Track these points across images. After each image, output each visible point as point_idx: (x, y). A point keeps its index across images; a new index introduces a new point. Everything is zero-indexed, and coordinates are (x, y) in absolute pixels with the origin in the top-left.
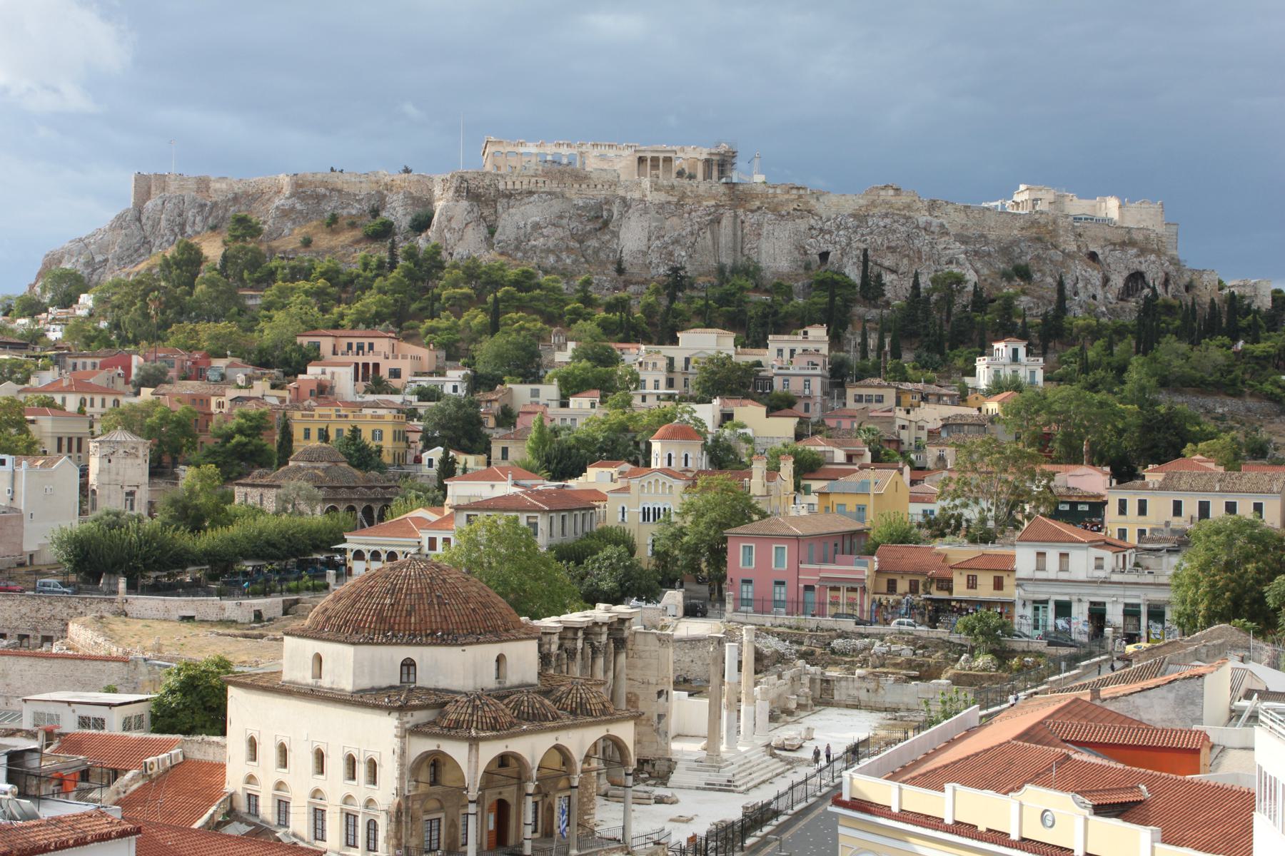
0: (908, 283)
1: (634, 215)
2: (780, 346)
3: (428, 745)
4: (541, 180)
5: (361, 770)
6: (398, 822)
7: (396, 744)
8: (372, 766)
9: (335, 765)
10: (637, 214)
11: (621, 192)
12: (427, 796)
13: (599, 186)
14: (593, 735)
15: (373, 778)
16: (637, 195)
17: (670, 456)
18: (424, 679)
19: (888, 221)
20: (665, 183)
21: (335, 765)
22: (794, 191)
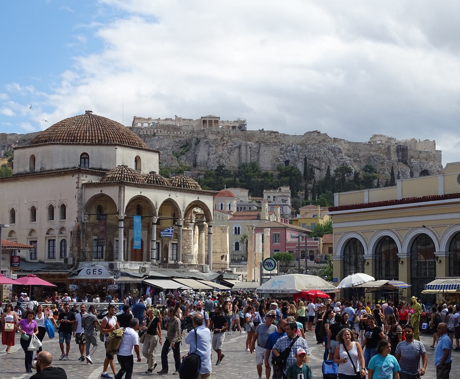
0: (324, 173)
1: (202, 144)
2: (269, 195)
3: (96, 191)
4: (159, 130)
5: (57, 212)
6: (79, 238)
7: (76, 192)
8: (63, 207)
9: (43, 213)
11: (195, 135)
12: (94, 226)
14: (190, 199)
15: (64, 216)
16: (202, 136)
17: (222, 204)
18: (93, 163)
19: (315, 146)
20: (215, 130)
21: (43, 213)
22: (273, 134)
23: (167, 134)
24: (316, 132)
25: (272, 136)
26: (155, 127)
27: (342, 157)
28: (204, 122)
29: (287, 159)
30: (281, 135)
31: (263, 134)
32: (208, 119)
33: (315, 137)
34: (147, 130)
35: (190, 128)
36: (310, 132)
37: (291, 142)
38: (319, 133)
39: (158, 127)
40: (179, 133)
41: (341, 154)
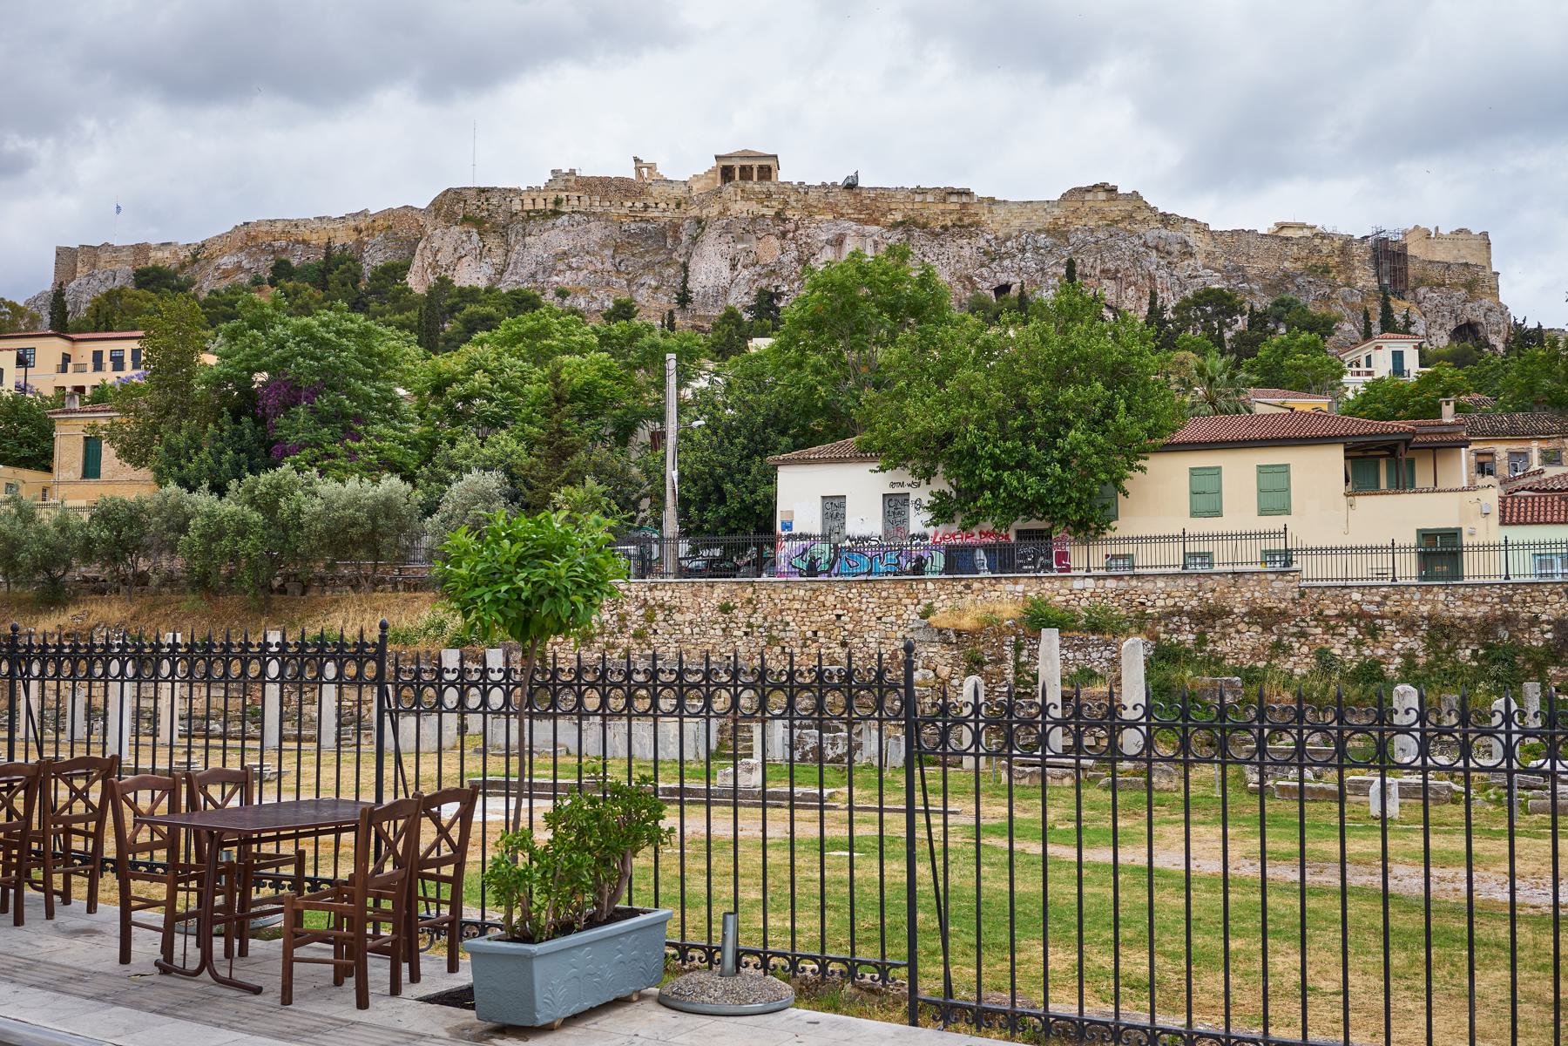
1: (711, 235)
10: (714, 234)
13: (662, 205)
20: (757, 188)
22: (954, 198)
23: (599, 210)
24: (1103, 187)
25: (952, 207)
26: (561, 184)
27: (1195, 269)
28: (727, 173)
29: (1003, 278)
30: (981, 201)
31: (918, 198)
32: (737, 164)
33: (1098, 205)
34: (534, 194)
35: (679, 192)
36: (1079, 190)
37: (1016, 223)
38: (1113, 190)
39: (572, 184)
40: (639, 205)
41: (1192, 262)
